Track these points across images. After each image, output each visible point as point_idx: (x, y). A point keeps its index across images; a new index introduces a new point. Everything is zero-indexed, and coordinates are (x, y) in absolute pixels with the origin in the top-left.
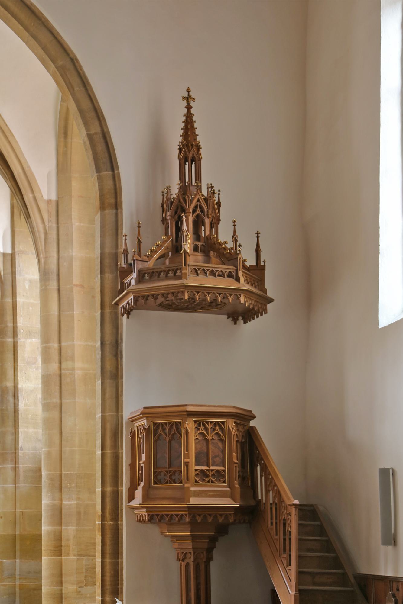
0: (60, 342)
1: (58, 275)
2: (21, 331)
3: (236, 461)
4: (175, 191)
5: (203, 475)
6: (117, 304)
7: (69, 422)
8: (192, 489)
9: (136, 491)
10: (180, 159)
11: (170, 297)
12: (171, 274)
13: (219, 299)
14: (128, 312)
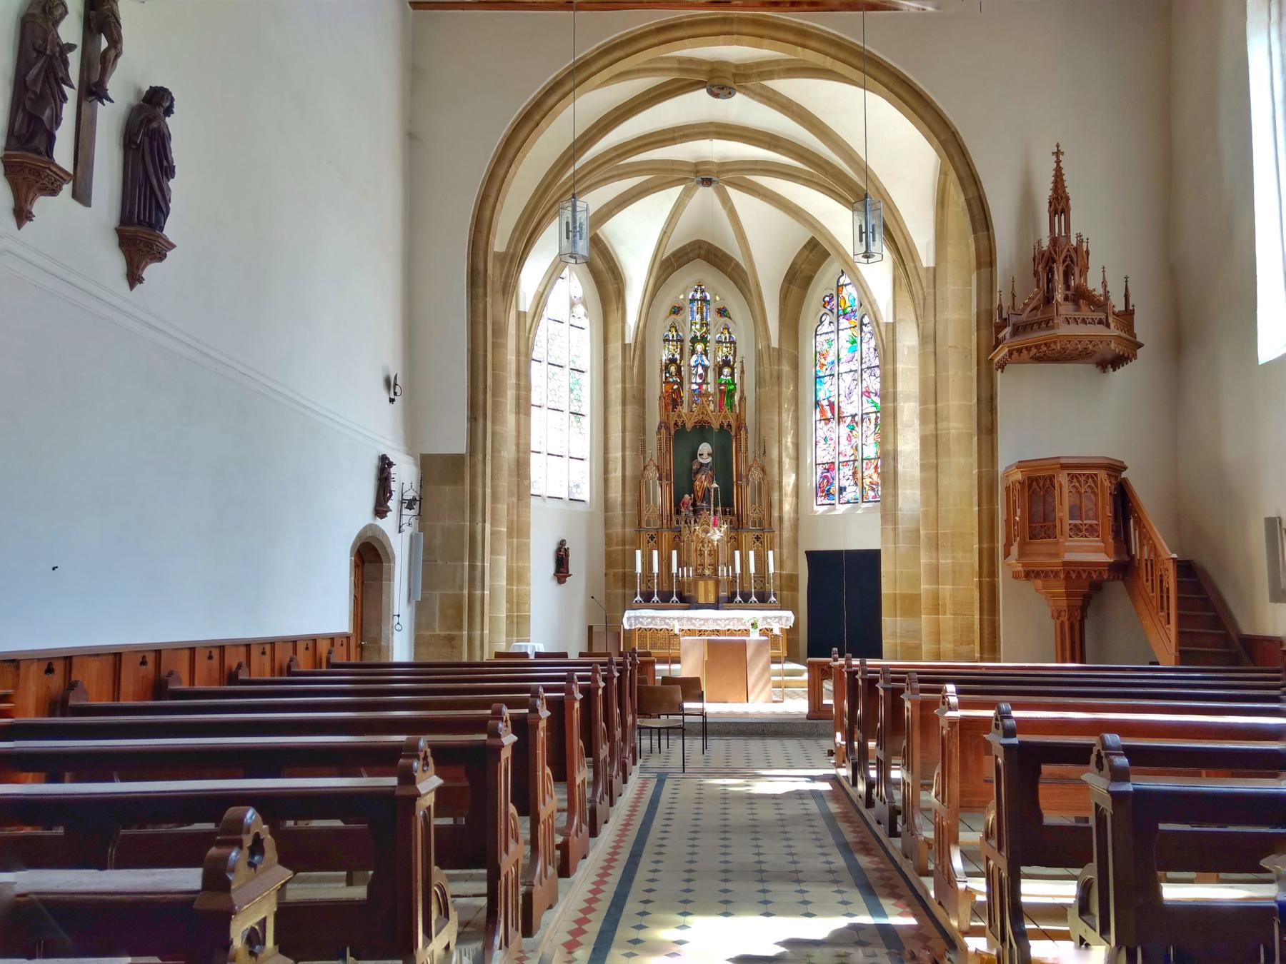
0: (936, 403)
2: (900, 396)
4: (1046, 243)
5: (1076, 530)
7: (945, 481)
11: (1044, 348)
12: (1043, 325)
13: (1090, 347)
14: (1002, 366)
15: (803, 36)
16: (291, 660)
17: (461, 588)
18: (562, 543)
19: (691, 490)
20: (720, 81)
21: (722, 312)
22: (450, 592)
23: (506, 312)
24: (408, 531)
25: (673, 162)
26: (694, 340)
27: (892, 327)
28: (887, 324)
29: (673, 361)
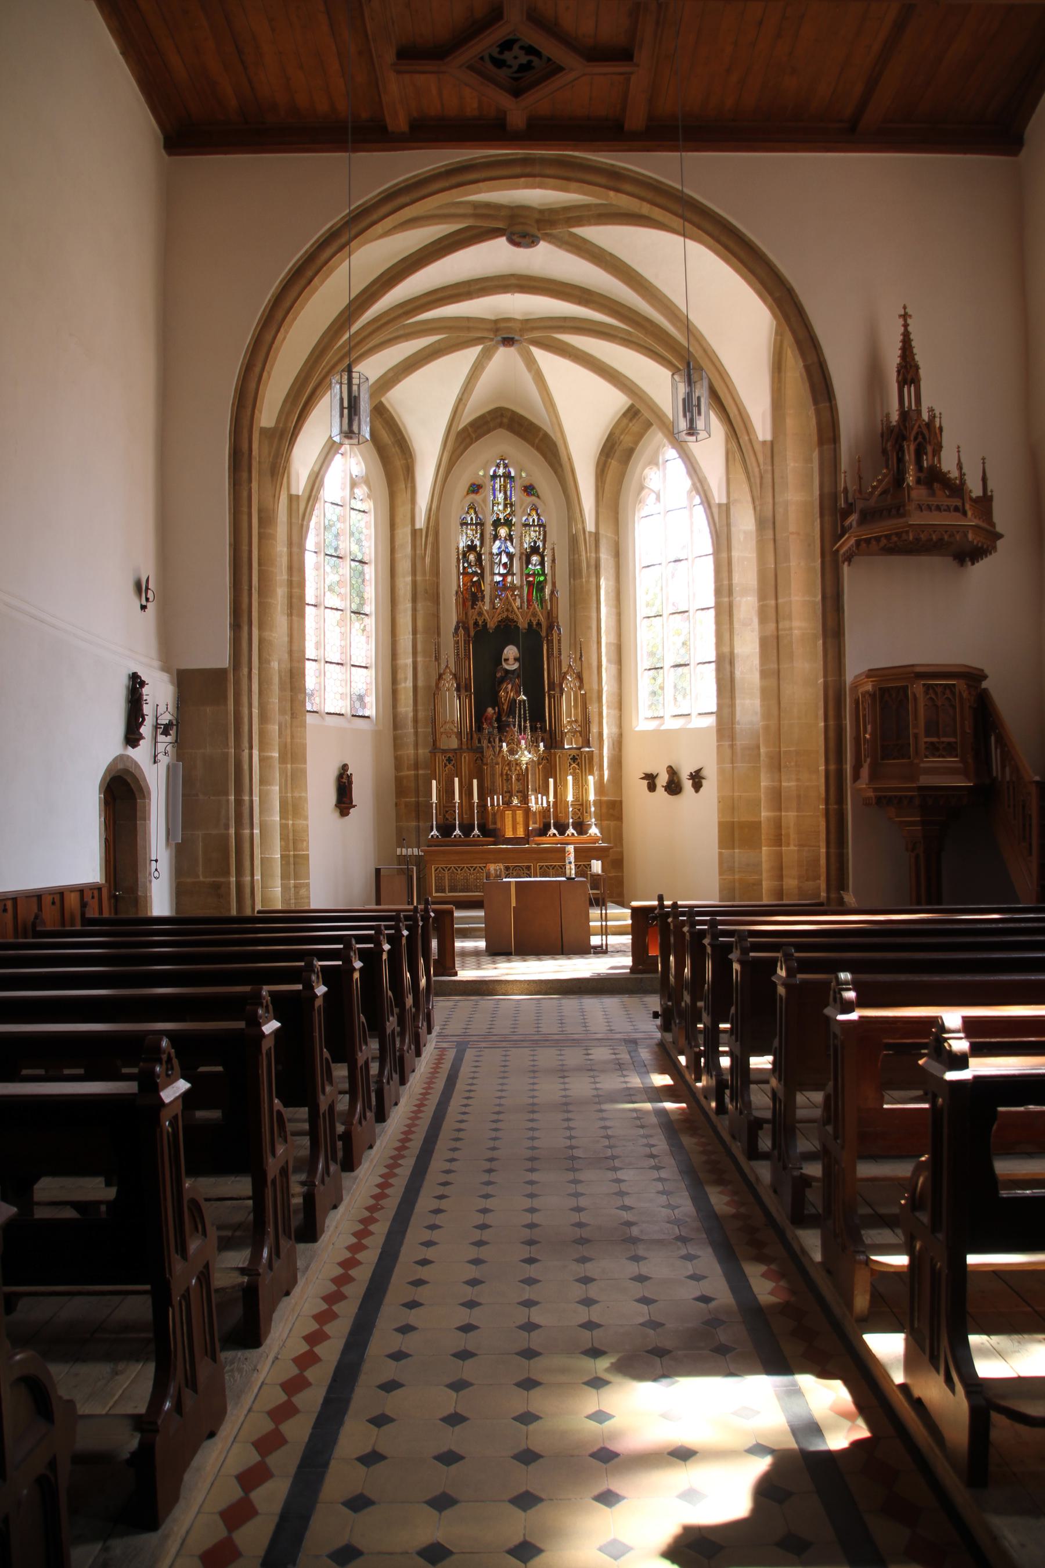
0: (776, 599)
1: (774, 523)
2: (736, 589)
3: (968, 731)
4: (895, 417)
5: (934, 749)
6: (837, 551)
8: (922, 765)
9: (862, 770)
10: (898, 382)
11: (894, 539)
13: (946, 537)
14: (849, 558)
15: (615, 179)
16: (36, 917)
17: (227, 827)
18: (345, 767)
19: (495, 702)
20: (522, 228)
21: (529, 490)
22: (214, 832)
23: (276, 497)
24: (164, 760)
25: (468, 319)
26: (497, 523)
27: (726, 509)
28: (720, 505)
29: (471, 548)
